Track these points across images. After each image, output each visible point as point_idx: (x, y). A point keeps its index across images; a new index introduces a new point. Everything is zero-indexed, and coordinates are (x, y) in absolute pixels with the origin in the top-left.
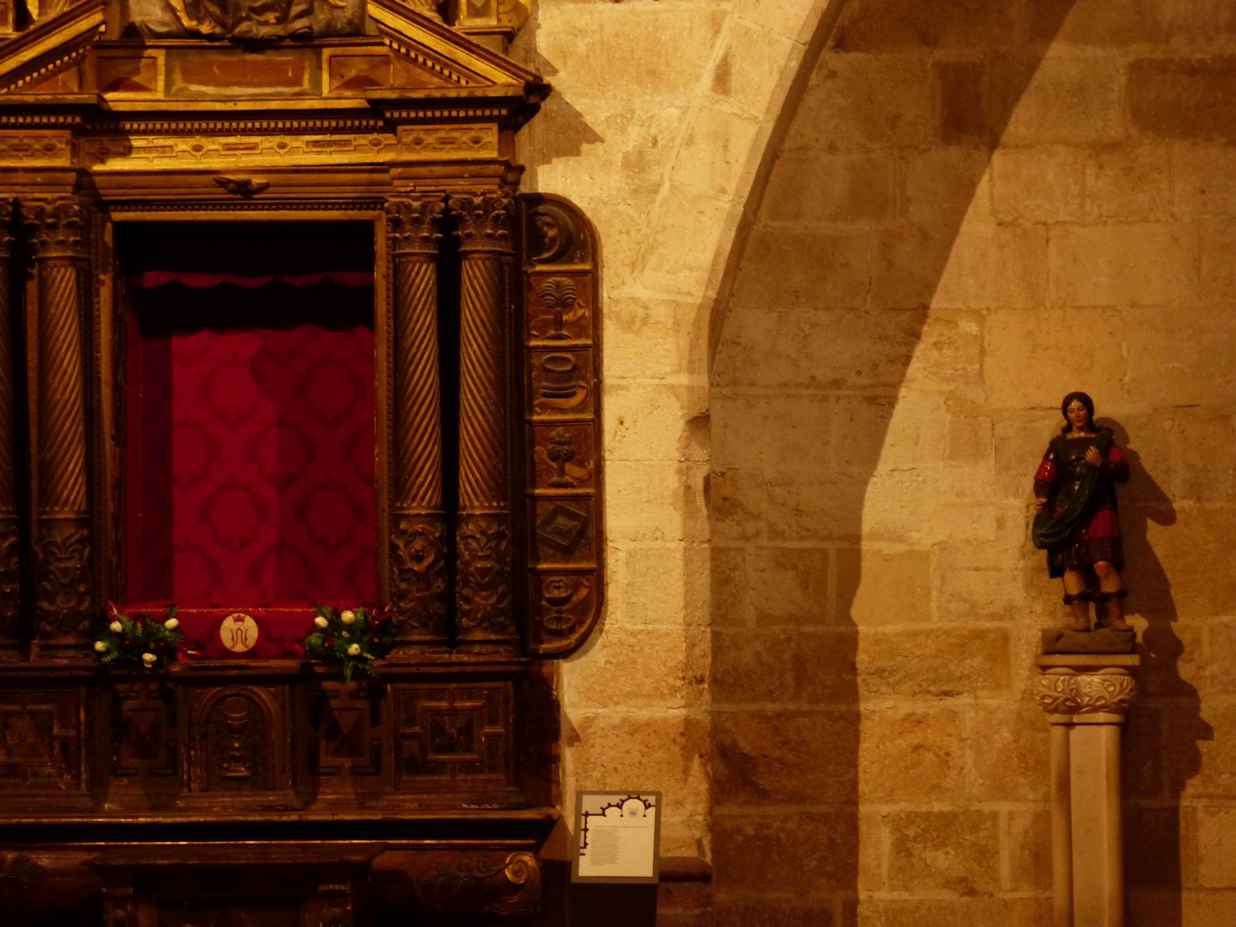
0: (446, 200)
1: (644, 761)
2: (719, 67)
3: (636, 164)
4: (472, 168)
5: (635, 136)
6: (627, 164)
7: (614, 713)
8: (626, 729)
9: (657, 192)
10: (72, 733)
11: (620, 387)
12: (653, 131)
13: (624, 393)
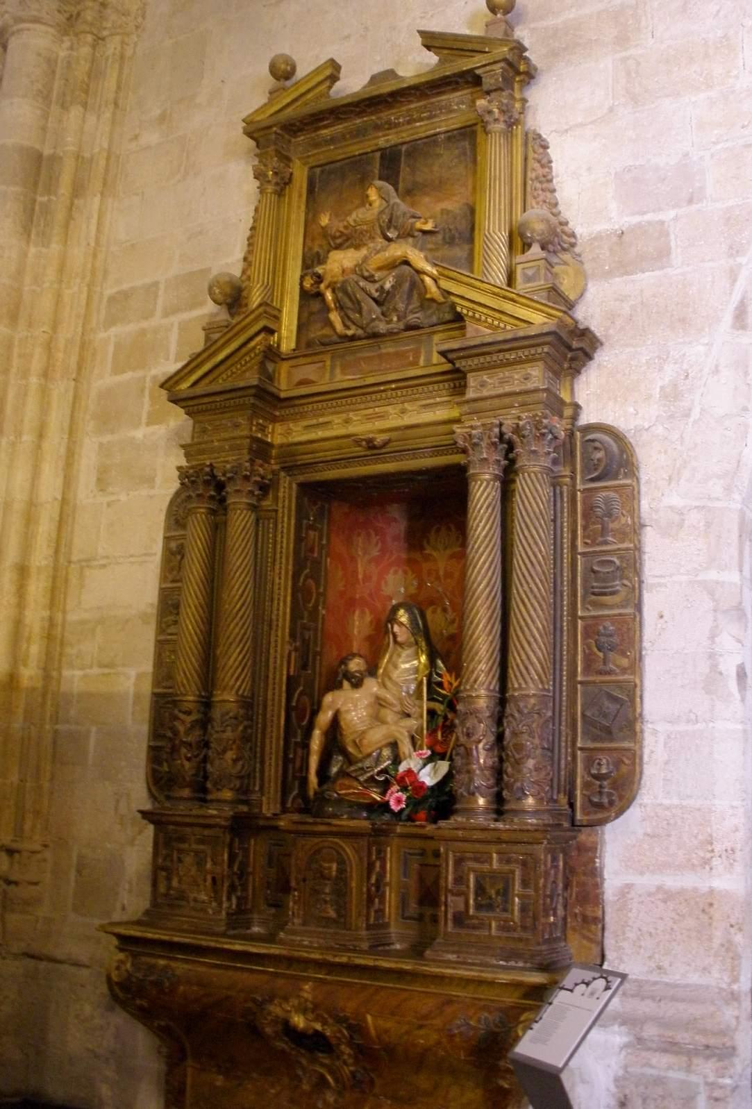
0: (501, 425)
1: (675, 927)
2: (736, 308)
3: (672, 394)
4: (520, 398)
5: (670, 371)
6: (664, 395)
7: (647, 881)
8: (660, 896)
9: (688, 416)
10: (218, 870)
11: (660, 585)
12: (685, 366)
13: (663, 589)
